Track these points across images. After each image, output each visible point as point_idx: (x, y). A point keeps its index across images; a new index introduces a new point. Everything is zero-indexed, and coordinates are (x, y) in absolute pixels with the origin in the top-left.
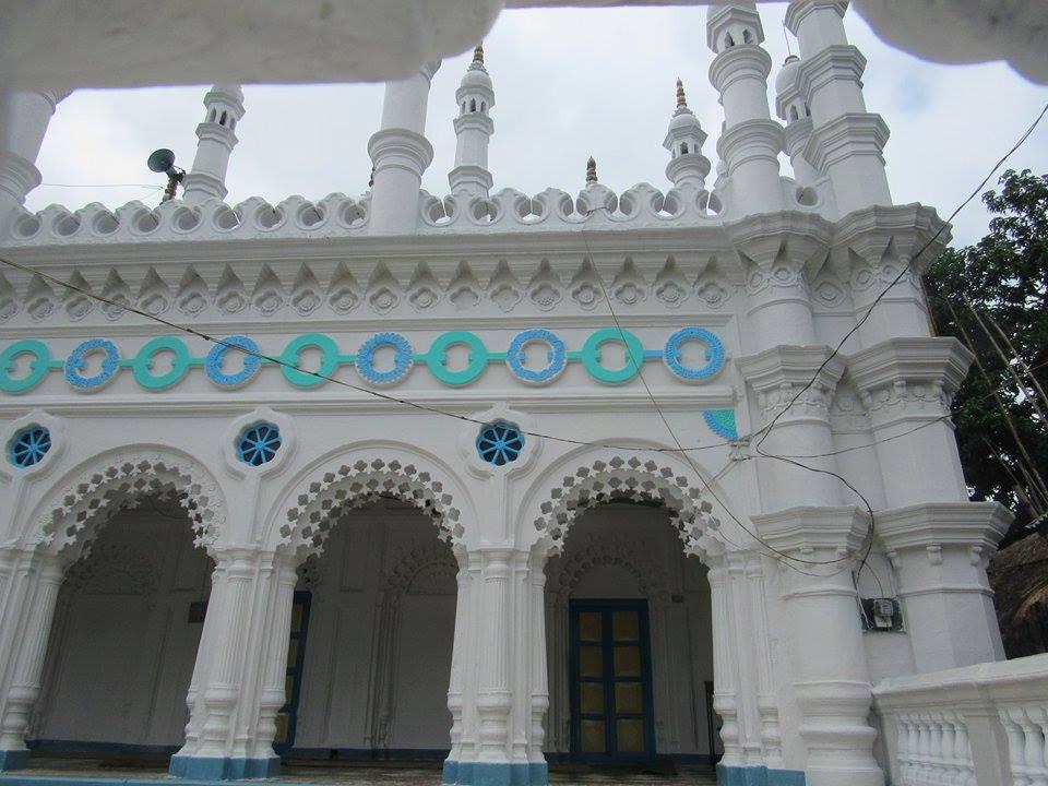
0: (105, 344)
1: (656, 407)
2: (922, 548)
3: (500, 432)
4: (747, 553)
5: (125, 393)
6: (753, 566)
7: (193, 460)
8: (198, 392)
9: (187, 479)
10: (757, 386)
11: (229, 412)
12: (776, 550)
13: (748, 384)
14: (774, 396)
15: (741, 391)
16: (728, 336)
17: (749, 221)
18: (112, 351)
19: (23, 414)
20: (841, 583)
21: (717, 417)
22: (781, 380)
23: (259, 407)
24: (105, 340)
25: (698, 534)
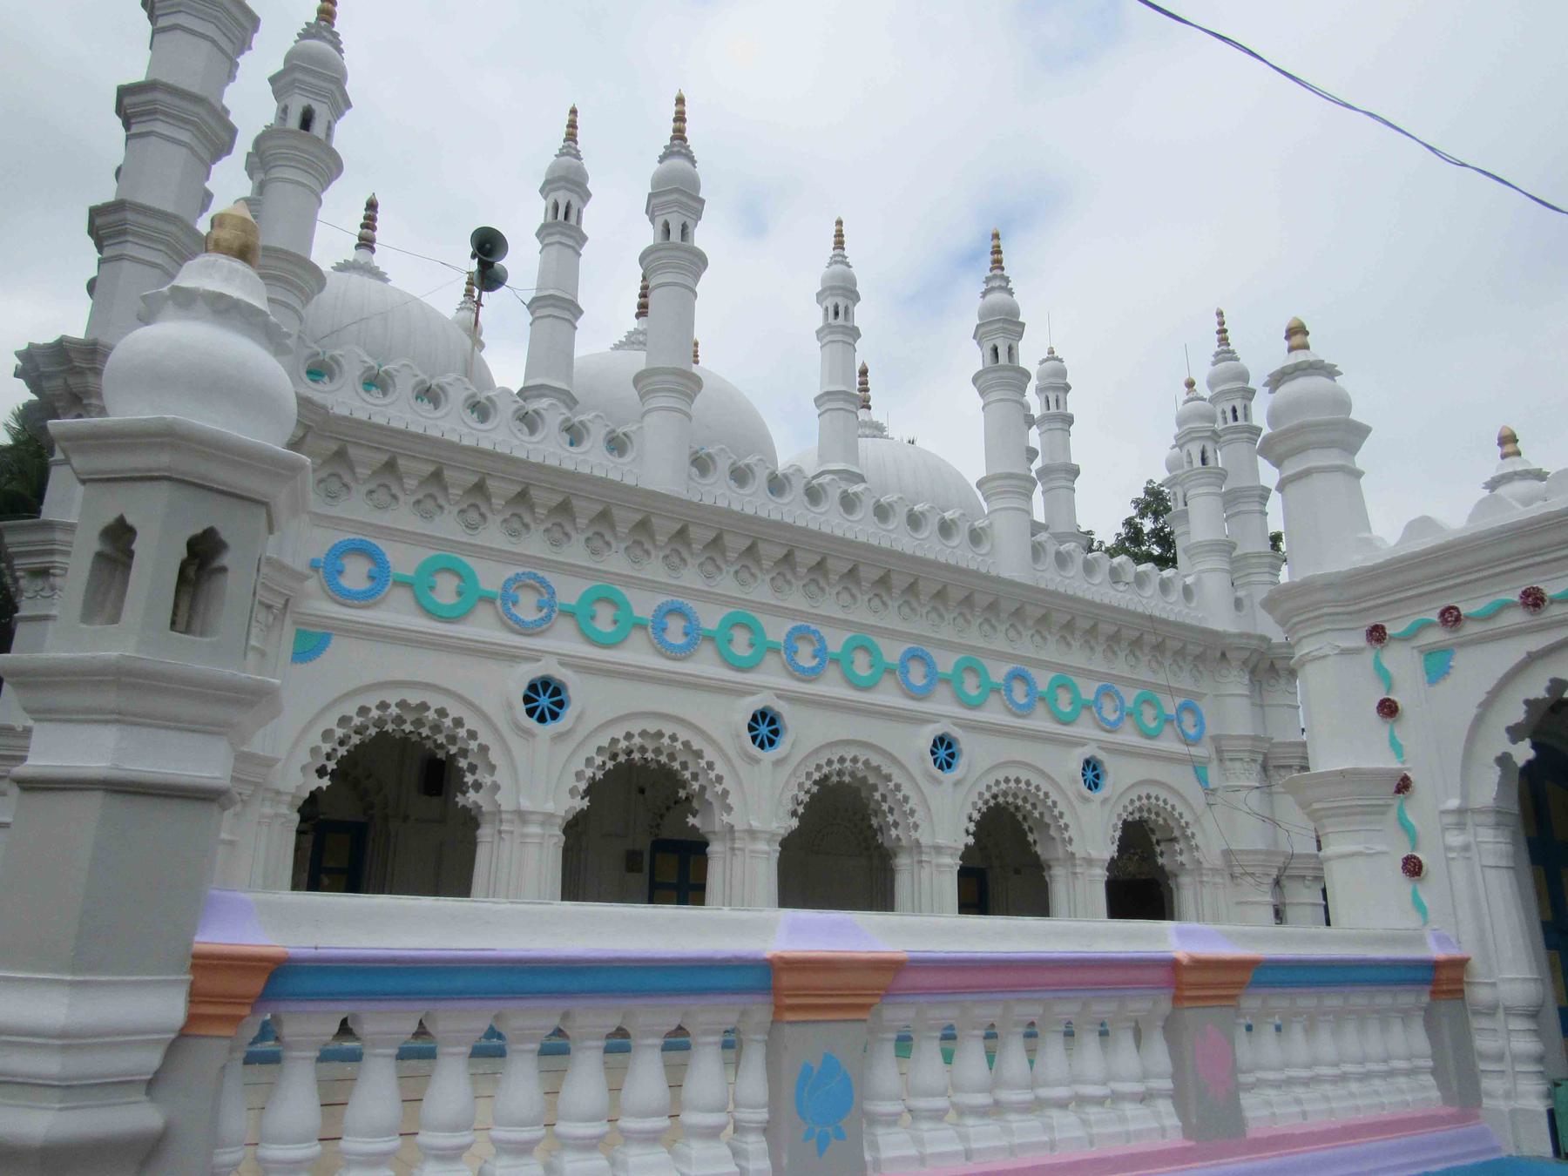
0: (815, 632)
1: (1170, 758)
2: (1304, 877)
3: (1094, 769)
4: (1215, 871)
5: (831, 687)
6: (1218, 880)
7: (894, 760)
8: (888, 696)
9: (888, 778)
10: (1227, 755)
11: (920, 720)
12: (1233, 867)
13: (1219, 751)
14: (1238, 765)
15: (1214, 756)
16: (1204, 705)
17: (1241, 635)
18: (821, 639)
19: (753, 694)
20: (1269, 898)
21: (1198, 768)
22: (1245, 756)
23: (945, 720)
24: (813, 627)
25: (1181, 853)
